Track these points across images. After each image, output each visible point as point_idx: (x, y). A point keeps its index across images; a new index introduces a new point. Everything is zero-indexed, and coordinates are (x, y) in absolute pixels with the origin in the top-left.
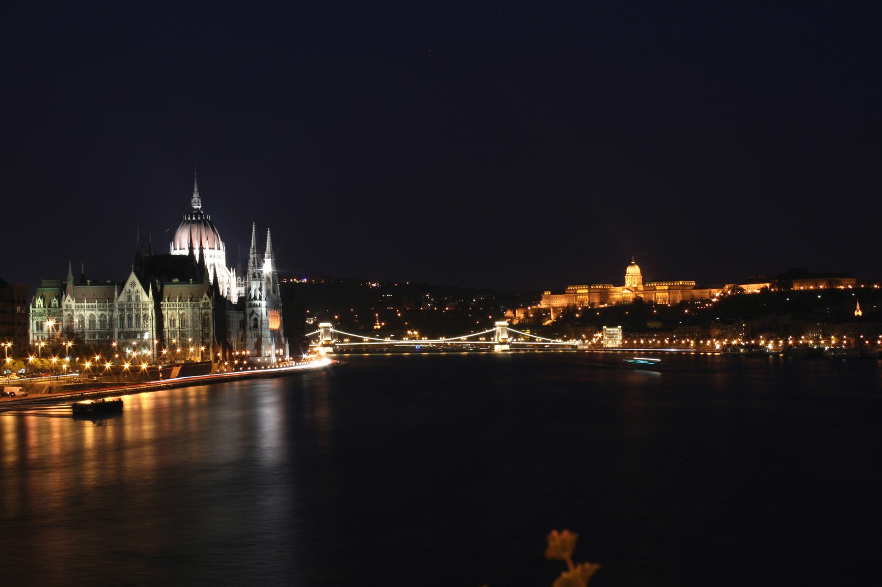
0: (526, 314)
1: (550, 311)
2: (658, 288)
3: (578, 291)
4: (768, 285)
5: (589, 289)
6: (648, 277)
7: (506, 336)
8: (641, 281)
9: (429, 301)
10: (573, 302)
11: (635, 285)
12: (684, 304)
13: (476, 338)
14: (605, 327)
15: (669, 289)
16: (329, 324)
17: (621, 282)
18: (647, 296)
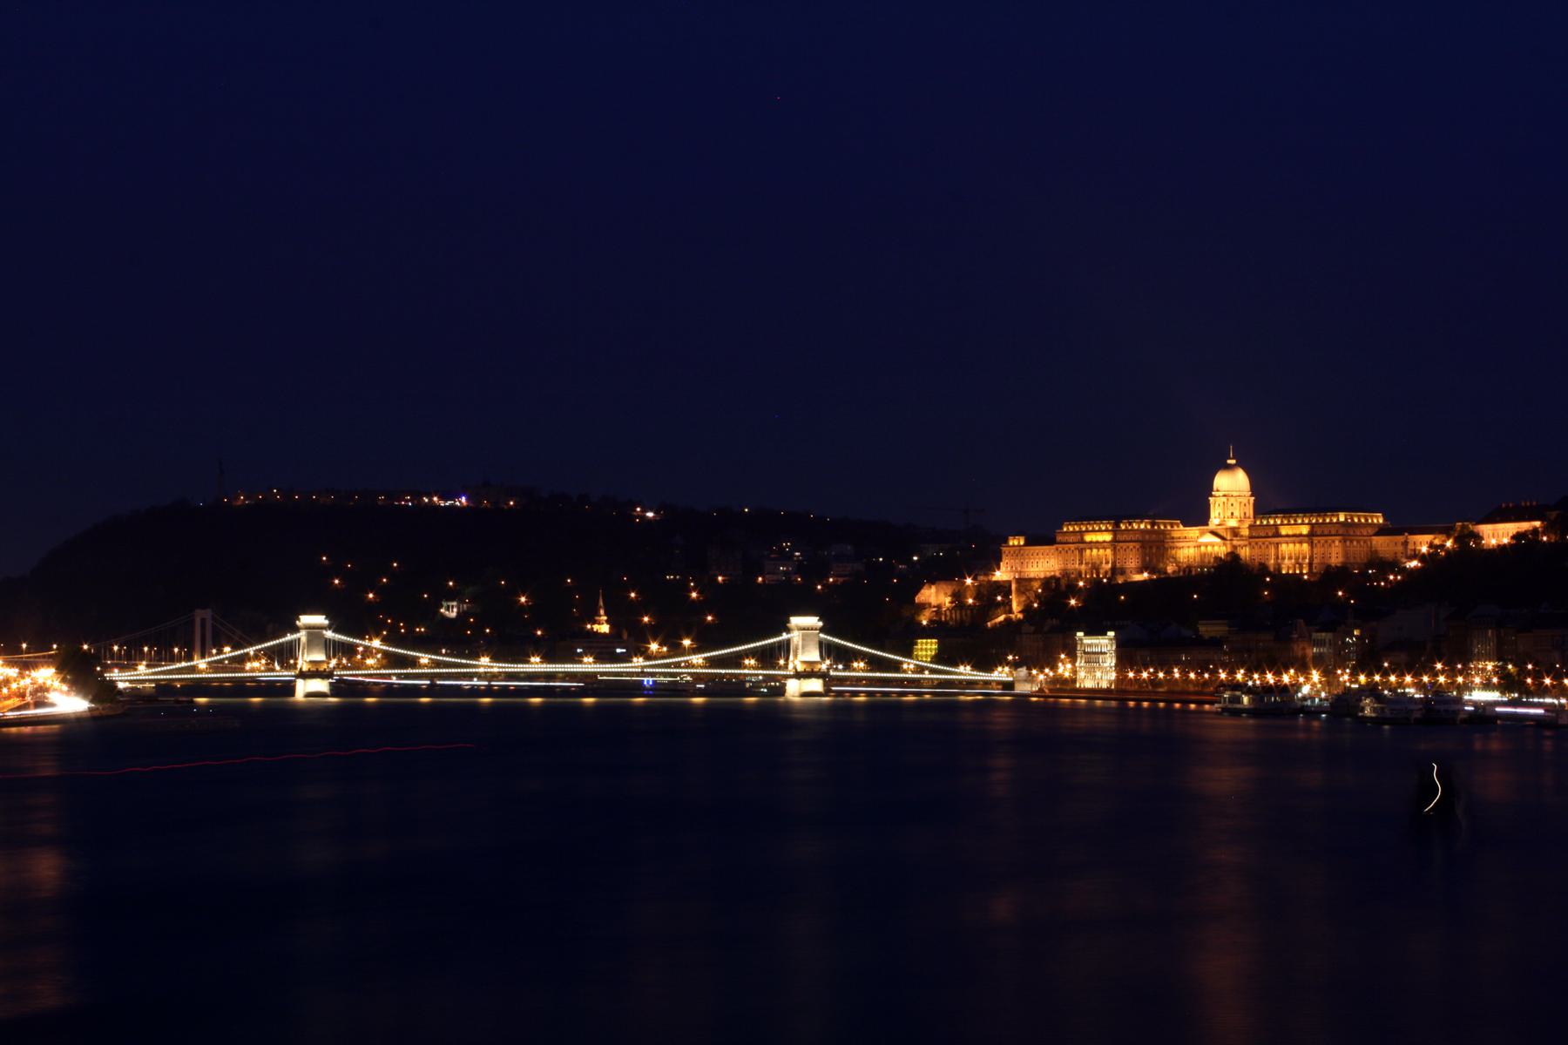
0: (958, 597)
1: (1010, 592)
2: (1284, 531)
3: (1088, 538)
4: (1537, 524)
5: (1115, 532)
6: (1266, 501)
7: (814, 655)
8: (1250, 512)
9: (786, 558)
10: (1075, 566)
11: (1233, 523)
12: (1331, 576)
13: (736, 661)
14: (1080, 634)
15: (1311, 535)
16: (320, 620)
17: (1198, 516)
18: (1257, 551)
